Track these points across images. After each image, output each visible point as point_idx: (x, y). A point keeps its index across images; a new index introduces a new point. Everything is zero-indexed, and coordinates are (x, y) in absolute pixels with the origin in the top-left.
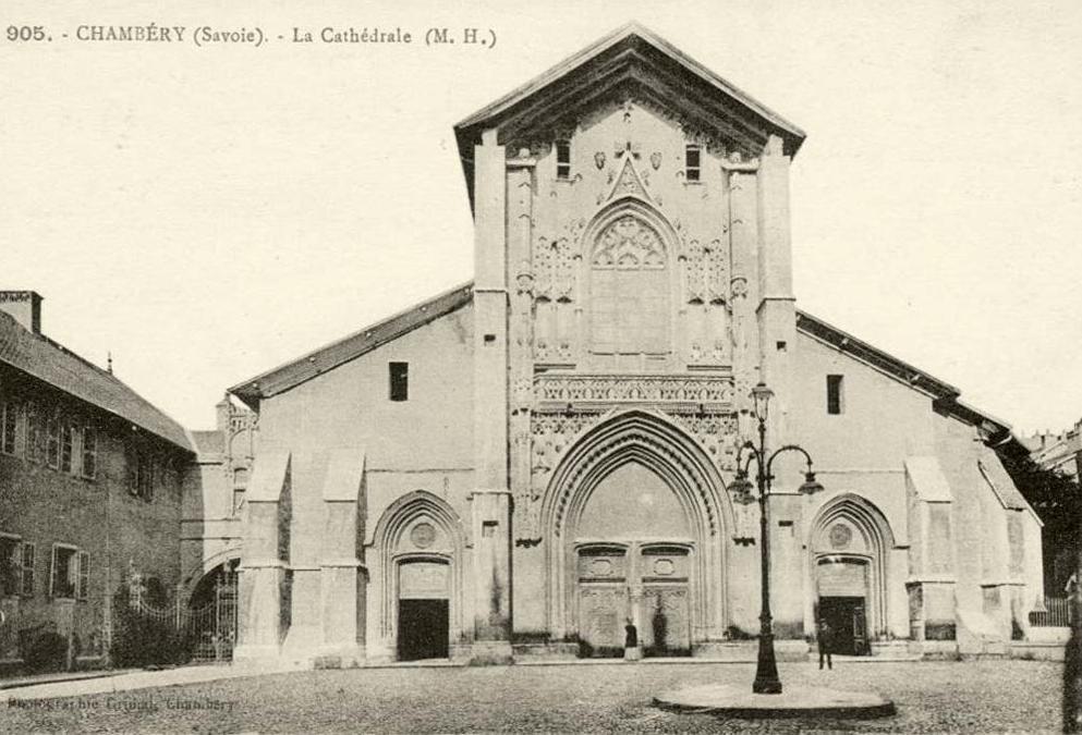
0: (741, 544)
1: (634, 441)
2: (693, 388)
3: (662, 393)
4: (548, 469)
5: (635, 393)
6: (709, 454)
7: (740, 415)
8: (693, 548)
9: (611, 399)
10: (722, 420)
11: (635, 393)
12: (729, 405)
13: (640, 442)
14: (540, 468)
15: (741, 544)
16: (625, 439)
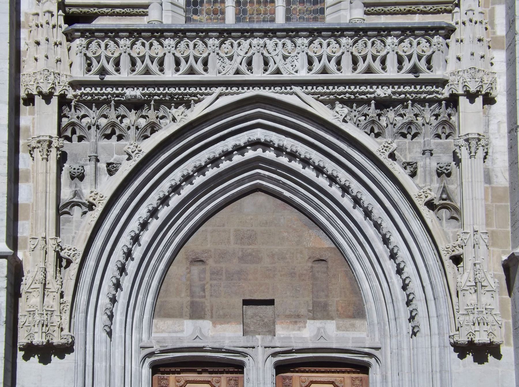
0: (470, 358)
1: (259, 152)
2: (370, 50)
3: (310, 62)
4: (91, 206)
5: (257, 62)
6: (402, 175)
7: (463, 101)
8: (377, 360)
9: (211, 76)
10: (428, 113)
11: (257, 62)
12: (442, 83)
13: (270, 155)
14: (78, 204)
15: (470, 358)
16: (240, 149)
